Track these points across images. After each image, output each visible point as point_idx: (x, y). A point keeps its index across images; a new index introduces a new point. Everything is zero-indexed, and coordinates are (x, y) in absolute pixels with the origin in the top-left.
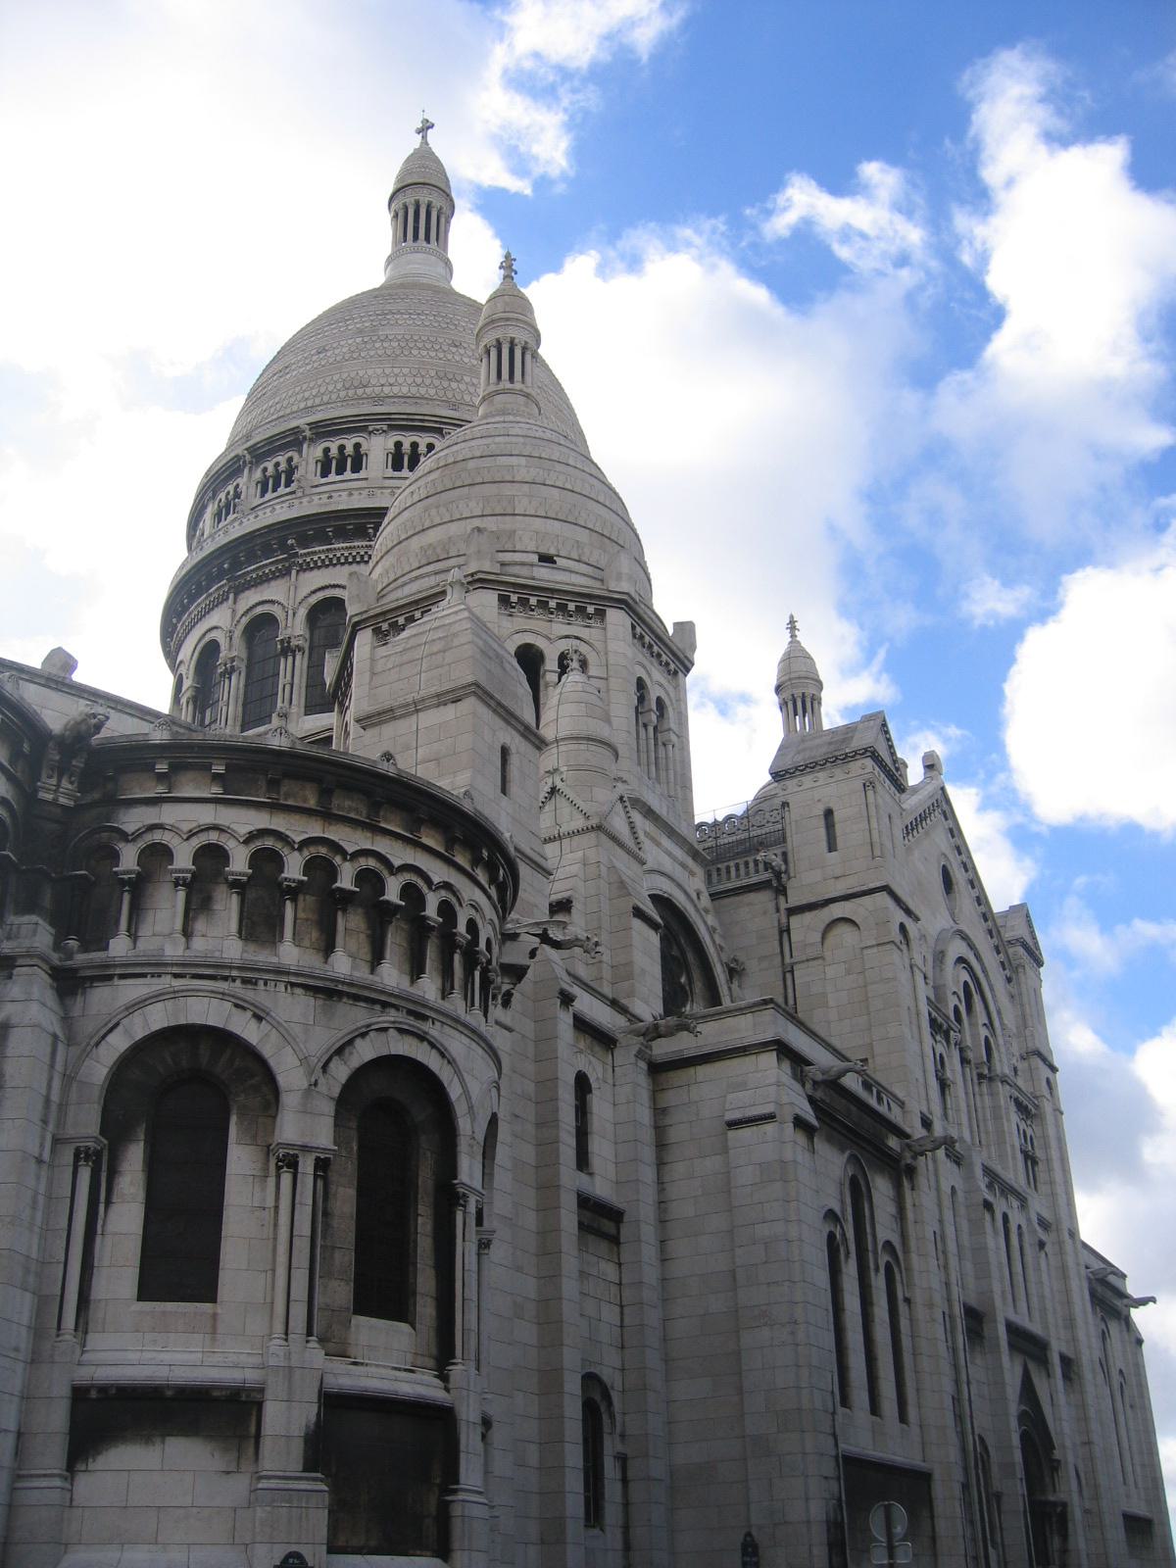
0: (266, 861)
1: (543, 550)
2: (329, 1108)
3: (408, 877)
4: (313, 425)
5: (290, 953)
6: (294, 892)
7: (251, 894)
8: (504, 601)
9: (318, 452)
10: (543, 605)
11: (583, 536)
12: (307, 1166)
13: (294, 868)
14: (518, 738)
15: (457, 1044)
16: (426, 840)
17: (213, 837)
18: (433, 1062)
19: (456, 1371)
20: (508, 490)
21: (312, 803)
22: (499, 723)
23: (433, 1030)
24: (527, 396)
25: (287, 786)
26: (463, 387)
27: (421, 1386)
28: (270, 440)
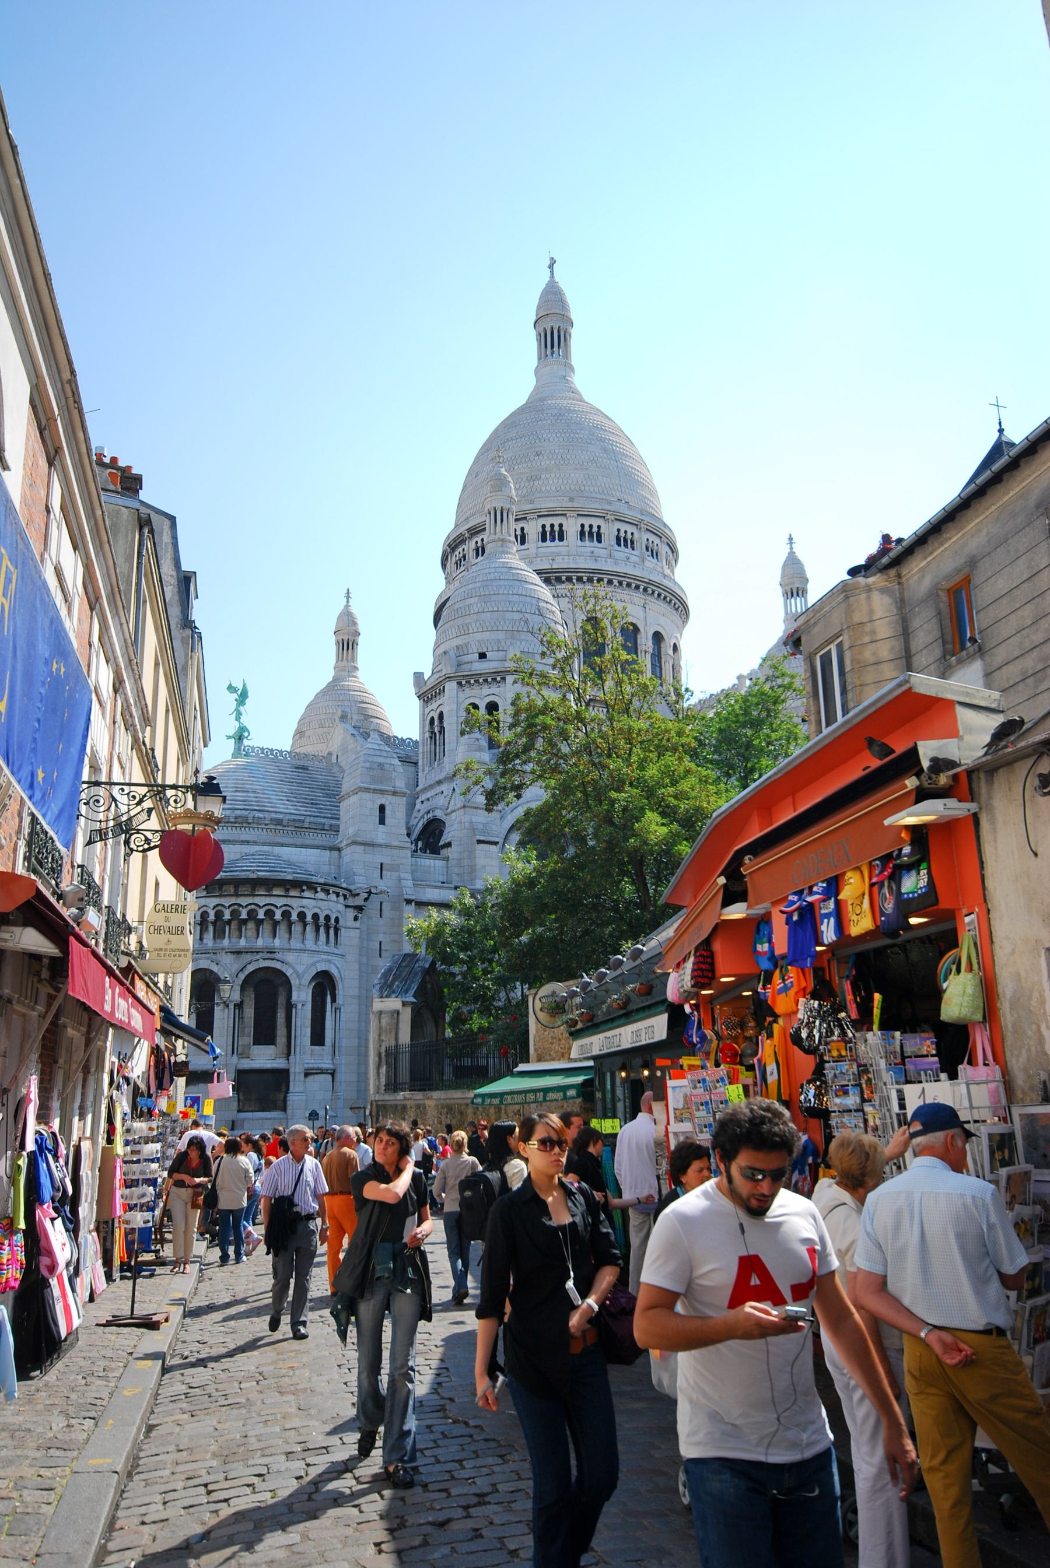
0: (219, 915)
1: (481, 651)
2: (239, 988)
3: (267, 907)
4: (469, 530)
5: (226, 942)
6: (229, 922)
7: (218, 924)
8: (460, 684)
9: (473, 545)
10: (477, 681)
11: (501, 635)
12: (232, 1006)
13: (227, 916)
14: (390, 797)
15: (290, 957)
16: (275, 892)
17: (204, 909)
18: (278, 965)
19: (292, 1057)
20: (468, 620)
21: (232, 892)
22: (377, 795)
23: (276, 956)
24: (503, 540)
25: (224, 887)
26: (541, 482)
27: (280, 1064)
28: (454, 540)
